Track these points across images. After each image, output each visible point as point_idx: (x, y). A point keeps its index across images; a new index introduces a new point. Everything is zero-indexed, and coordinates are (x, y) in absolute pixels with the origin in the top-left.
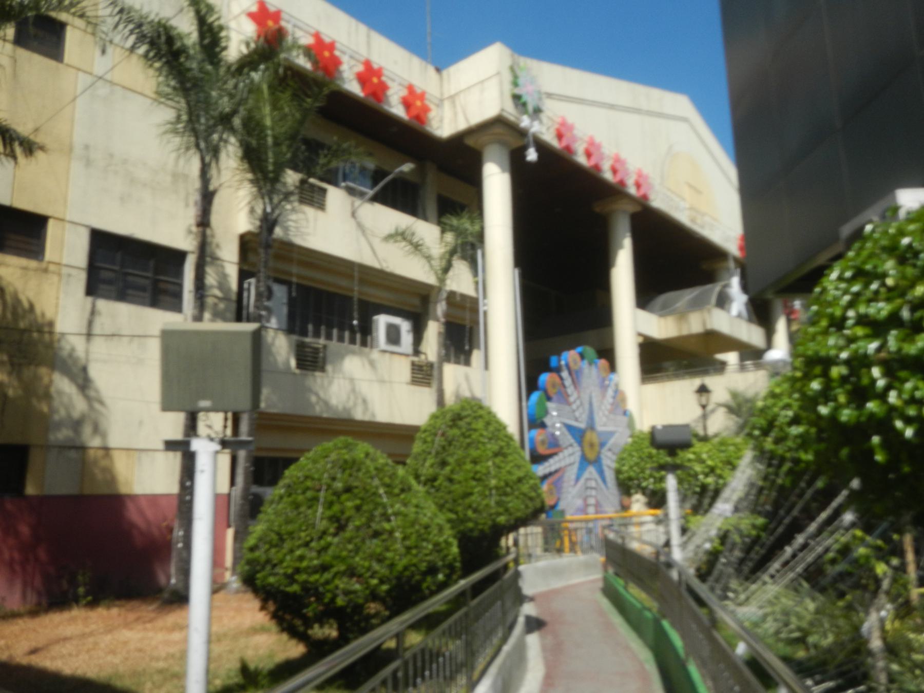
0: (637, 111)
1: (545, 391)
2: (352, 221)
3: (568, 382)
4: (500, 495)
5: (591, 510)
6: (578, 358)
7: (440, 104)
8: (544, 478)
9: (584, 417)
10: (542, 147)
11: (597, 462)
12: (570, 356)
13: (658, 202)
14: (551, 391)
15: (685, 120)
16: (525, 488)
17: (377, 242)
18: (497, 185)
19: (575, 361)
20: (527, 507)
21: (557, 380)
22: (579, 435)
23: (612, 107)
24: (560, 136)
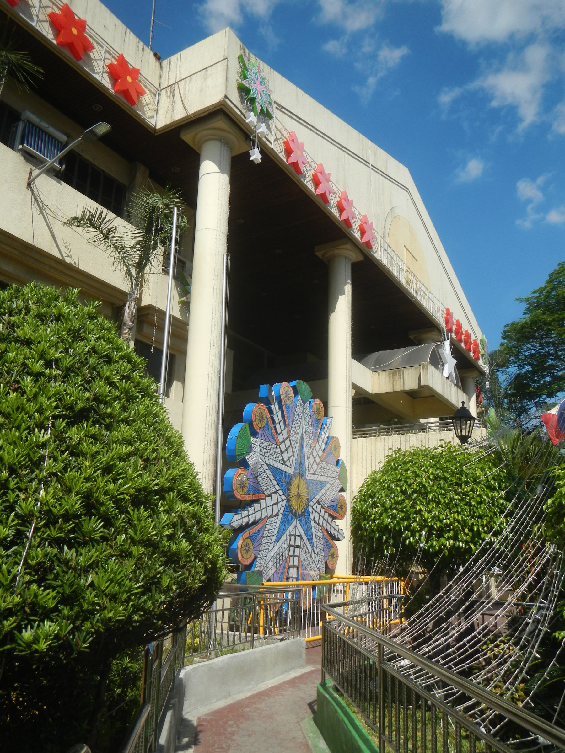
0: (366, 163)
1: (251, 424)
2: (29, 192)
3: (278, 417)
4: (58, 542)
5: (293, 572)
6: (292, 393)
7: (157, 93)
8: (241, 529)
9: (293, 460)
10: (265, 152)
11: (304, 515)
12: (284, 388)
13: (379, 254)
14: (257, 425)
15: (406, 189)
16: (153, 524)
17: (58, 228)
18: (214, 186)
19: (287, 394)
20: (152, 585)
21: (266, 412)
23: (342, 148)
24: (288, 152)
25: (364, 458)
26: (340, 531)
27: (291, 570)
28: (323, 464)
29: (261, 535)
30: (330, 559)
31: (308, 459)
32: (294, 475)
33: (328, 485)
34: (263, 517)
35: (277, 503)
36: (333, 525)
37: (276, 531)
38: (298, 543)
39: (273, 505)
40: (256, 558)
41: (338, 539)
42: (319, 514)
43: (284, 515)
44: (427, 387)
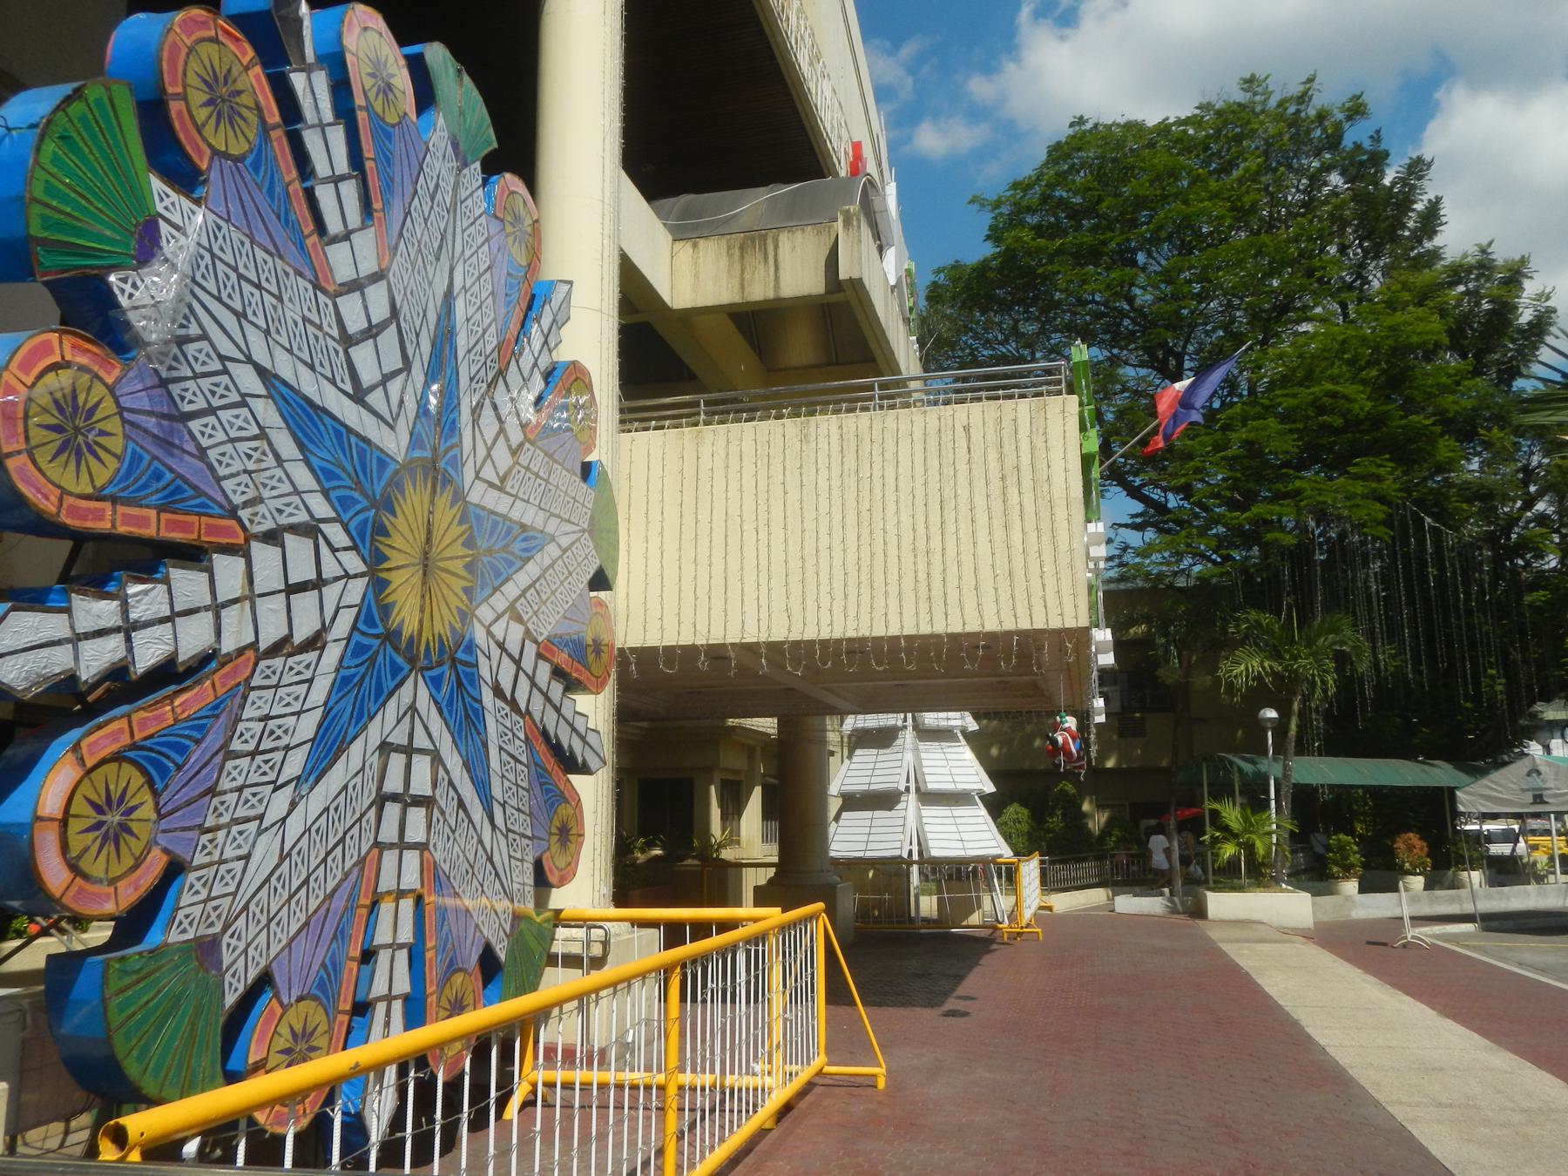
3: (328, 149)
22: (364, 493)
25: (655, 497)
26: (591, 738)
27: (386, 907)
28: (534, 457)
29: (213, 740)
30: (555, 848)
32: (409, 466)
33: (552, 550)
34: (228, 646)
35: (318, 584)
36: (567, 711)
37: (307, 726)
38: (421, 784)
39: (292, 589)
40: (175, 870)
41: (585, 770)
42: (517, 663)
43: (355, 649)
44: (857, 285)
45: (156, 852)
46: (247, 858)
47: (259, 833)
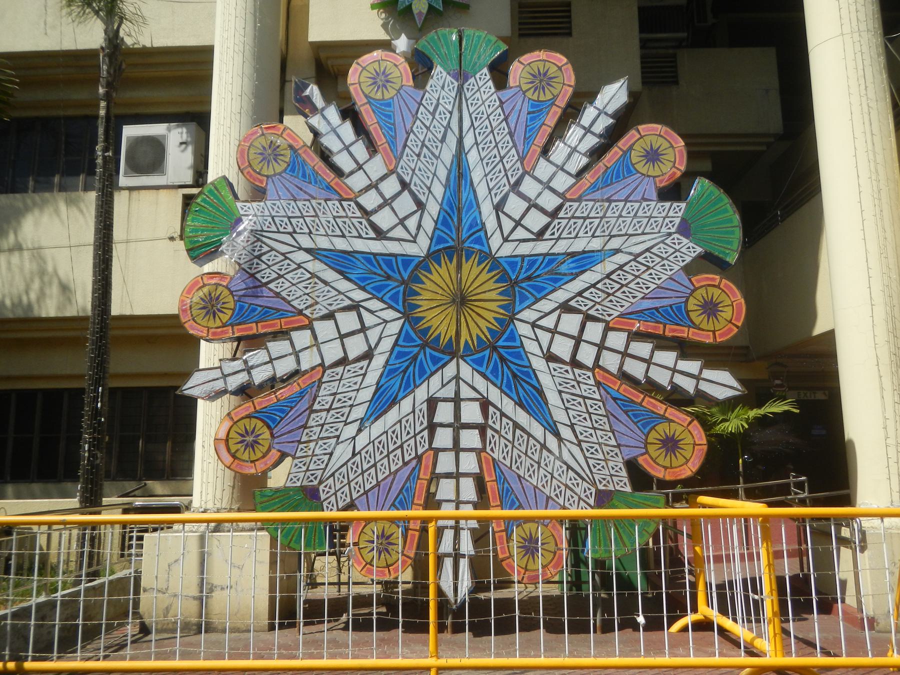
31: (499, 208)
37: (366, 395)
45: (273, 451)
46: (331, 454)
47: (337, 443)
